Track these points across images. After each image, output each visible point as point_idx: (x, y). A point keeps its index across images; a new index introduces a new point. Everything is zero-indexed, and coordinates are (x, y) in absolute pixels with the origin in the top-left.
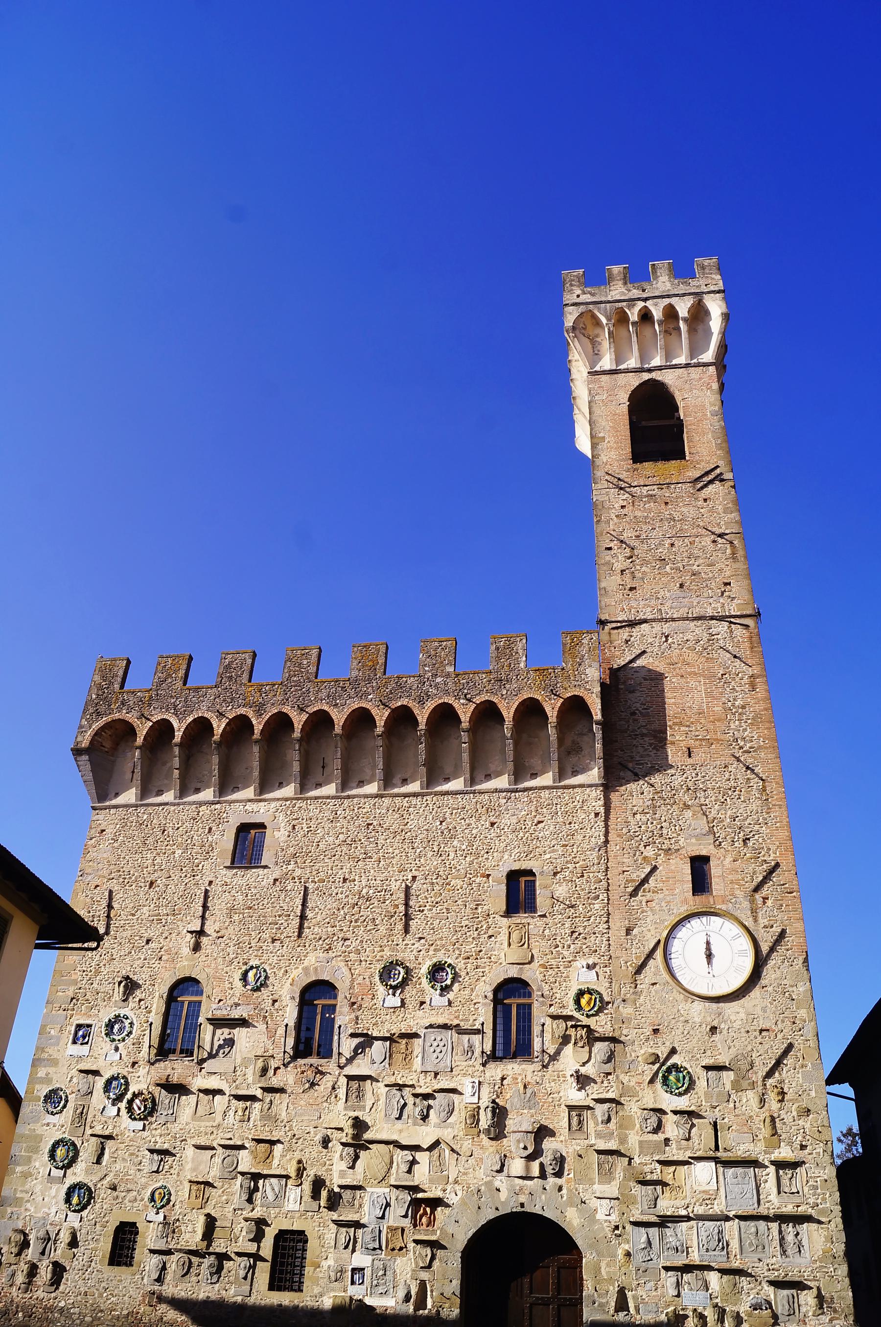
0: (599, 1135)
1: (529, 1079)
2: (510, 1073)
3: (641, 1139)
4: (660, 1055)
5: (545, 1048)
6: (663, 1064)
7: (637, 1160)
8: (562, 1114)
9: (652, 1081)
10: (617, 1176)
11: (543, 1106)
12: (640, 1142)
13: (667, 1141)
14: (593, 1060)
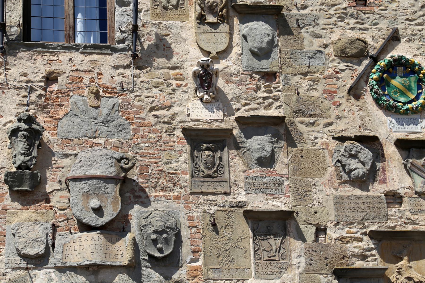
0: (252, 186)
1: (105, 80)
2: (65, 68)
3: (339, 193)
4: (370, 41)
5: (140, 23)
6: (375, 60)
7: (333, 233)
8: (178, 147)
9: (355, 92)
10: (295, 261)
11: (135, 132)
12: (338, 200)
13: (394, 198)
14: (236, 51)
